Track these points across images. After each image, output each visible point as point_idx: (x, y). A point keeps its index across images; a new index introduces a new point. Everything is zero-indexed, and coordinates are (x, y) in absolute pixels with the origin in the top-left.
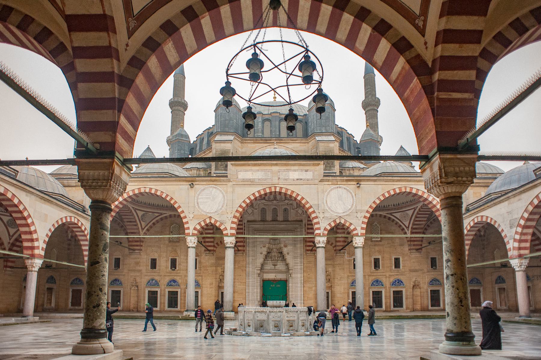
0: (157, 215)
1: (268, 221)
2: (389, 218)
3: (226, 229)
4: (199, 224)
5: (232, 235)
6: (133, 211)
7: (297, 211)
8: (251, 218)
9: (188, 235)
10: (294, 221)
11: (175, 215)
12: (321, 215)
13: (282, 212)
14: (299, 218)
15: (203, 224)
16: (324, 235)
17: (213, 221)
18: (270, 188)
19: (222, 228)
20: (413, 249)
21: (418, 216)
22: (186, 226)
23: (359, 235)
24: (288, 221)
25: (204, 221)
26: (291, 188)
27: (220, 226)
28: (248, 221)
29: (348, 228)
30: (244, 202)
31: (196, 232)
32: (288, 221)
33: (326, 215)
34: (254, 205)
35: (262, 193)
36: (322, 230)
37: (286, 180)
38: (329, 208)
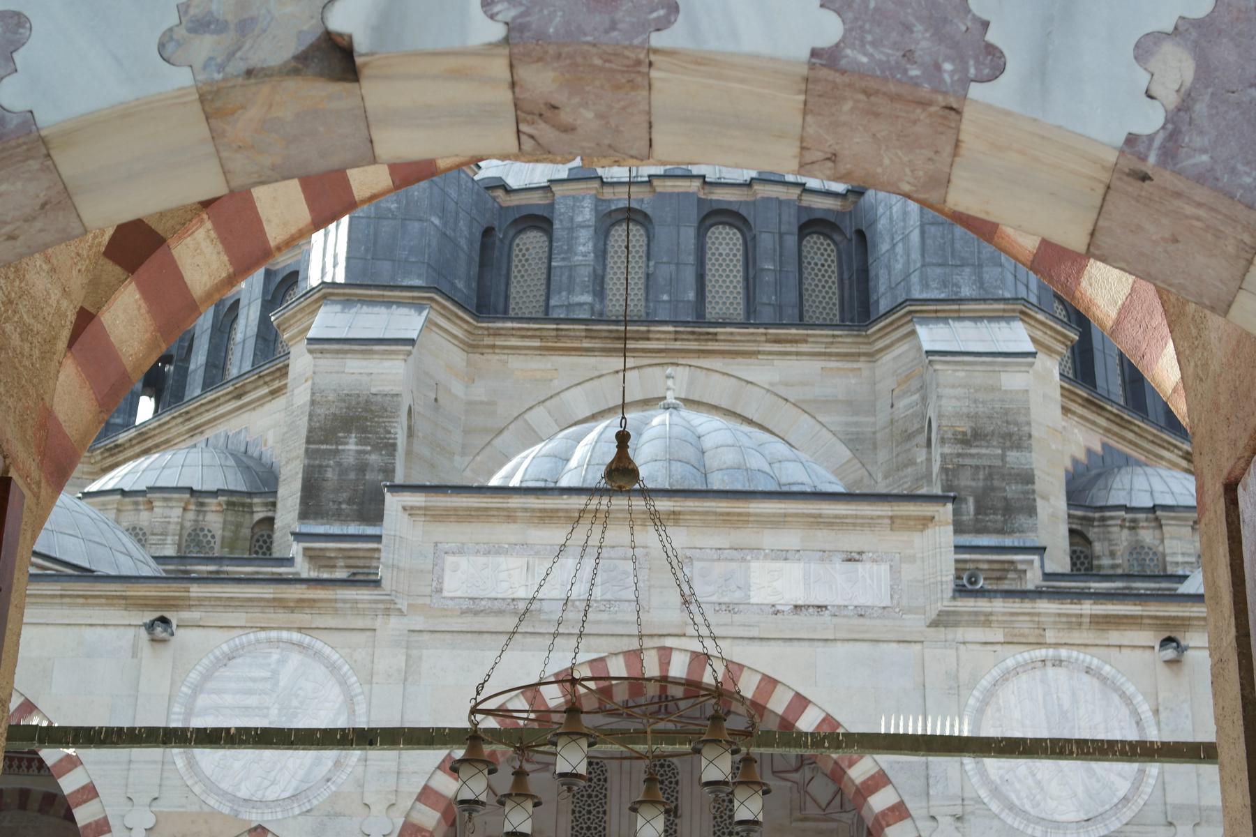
7: (803, 789)
11: (24, 794)
37: (729, 608)
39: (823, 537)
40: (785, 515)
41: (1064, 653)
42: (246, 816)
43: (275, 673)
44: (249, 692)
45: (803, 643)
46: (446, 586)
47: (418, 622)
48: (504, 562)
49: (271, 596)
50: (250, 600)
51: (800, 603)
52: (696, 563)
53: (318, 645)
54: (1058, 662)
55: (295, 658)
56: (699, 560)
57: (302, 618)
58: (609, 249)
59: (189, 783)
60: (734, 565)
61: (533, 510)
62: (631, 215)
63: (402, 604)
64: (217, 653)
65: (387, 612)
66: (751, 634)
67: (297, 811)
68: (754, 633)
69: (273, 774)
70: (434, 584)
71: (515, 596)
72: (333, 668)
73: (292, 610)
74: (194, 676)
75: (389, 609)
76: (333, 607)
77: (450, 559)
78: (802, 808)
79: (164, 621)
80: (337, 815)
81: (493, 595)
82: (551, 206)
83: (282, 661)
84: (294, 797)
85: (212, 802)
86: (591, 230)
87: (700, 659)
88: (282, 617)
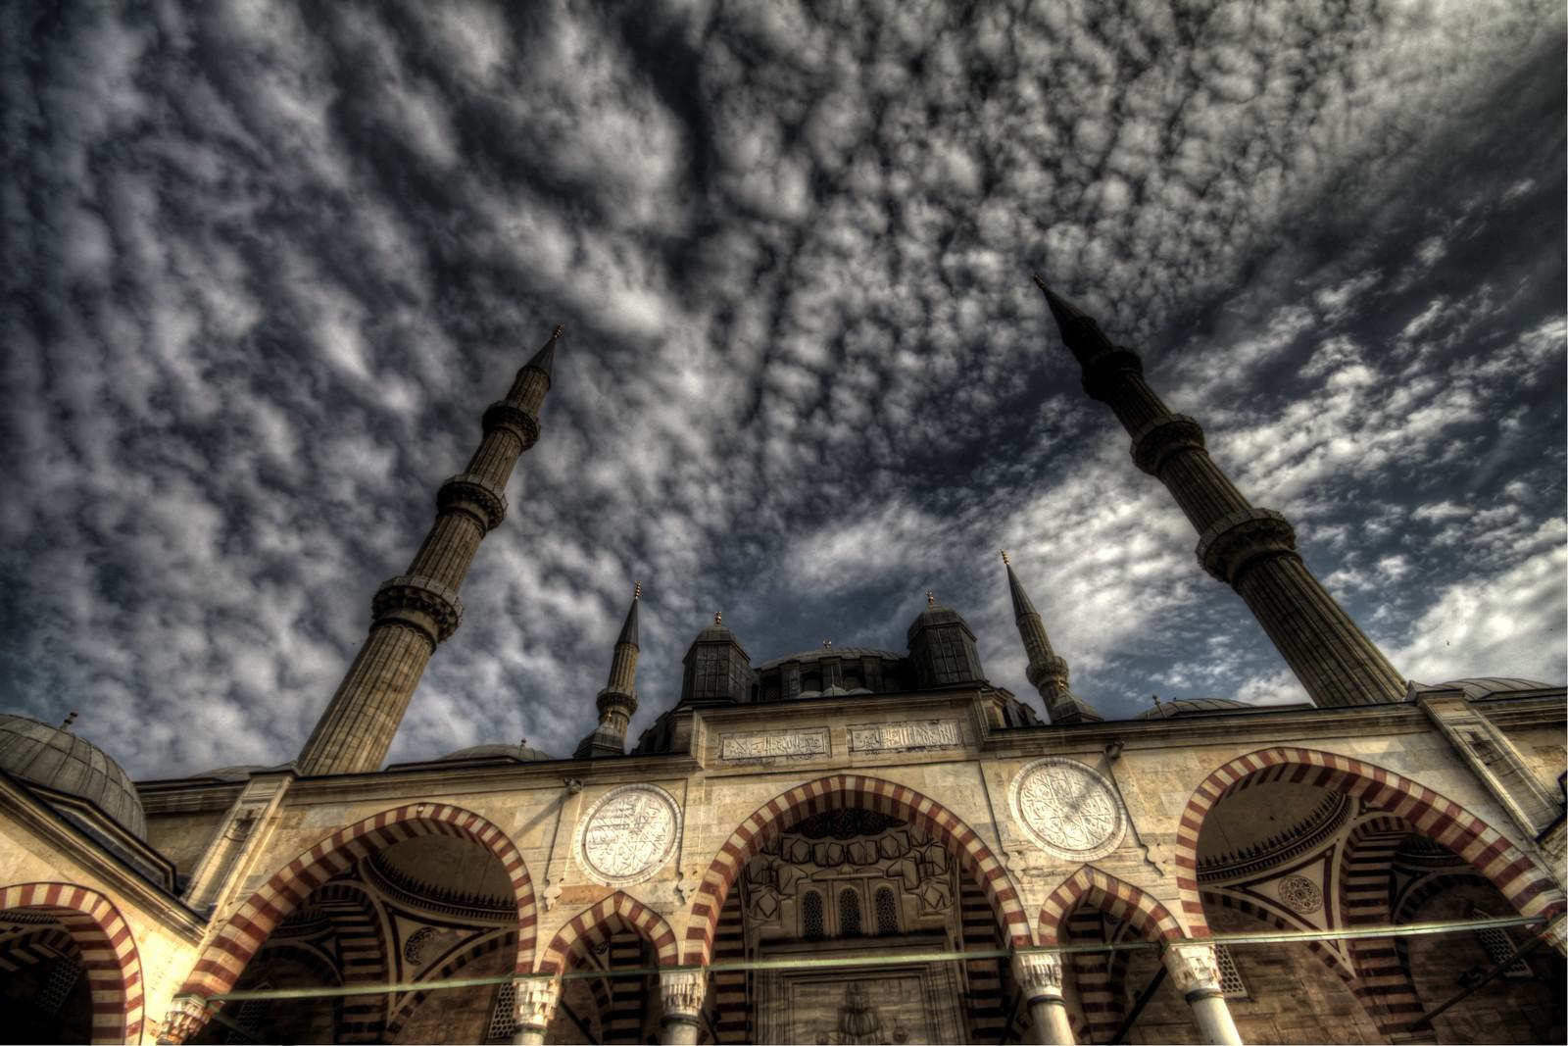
0: (463, 934)
1: (829, 939)
2: (1246, 907)
5: (694, 961)
6: (384, 919)
7: (922, 898)
8: (774, 929)
10: (915, 933)
12: (1016, 864)
13: (874, 905)
14: (930, 920)
15: (588, 921)
16: (1045, 946)
17: (626, 908)
18: (825, 781)
20: (1397, 1028)
21: (1353, 881)
23: (1188, 934)
24: (896, 934)
25: (596, 909)
26: (894, 775)
27: (649, 927)
29: (1132, 907)
32: (896, 934)
33: (1034, 860)
34: (782, 883)
35: (800, 796)
36: (1034, 923)
37: (874, 751)
38: (1038, 835)
41: (1056, 759)
43: (634, 806)
47: (711, 772)
54: (1054, 764)
57: (649, 776)
68: (888, 763)
72: (666, 800)
78: (924, 908)
83: (638, 799)
84: (641, 872)
88: (638, 777)
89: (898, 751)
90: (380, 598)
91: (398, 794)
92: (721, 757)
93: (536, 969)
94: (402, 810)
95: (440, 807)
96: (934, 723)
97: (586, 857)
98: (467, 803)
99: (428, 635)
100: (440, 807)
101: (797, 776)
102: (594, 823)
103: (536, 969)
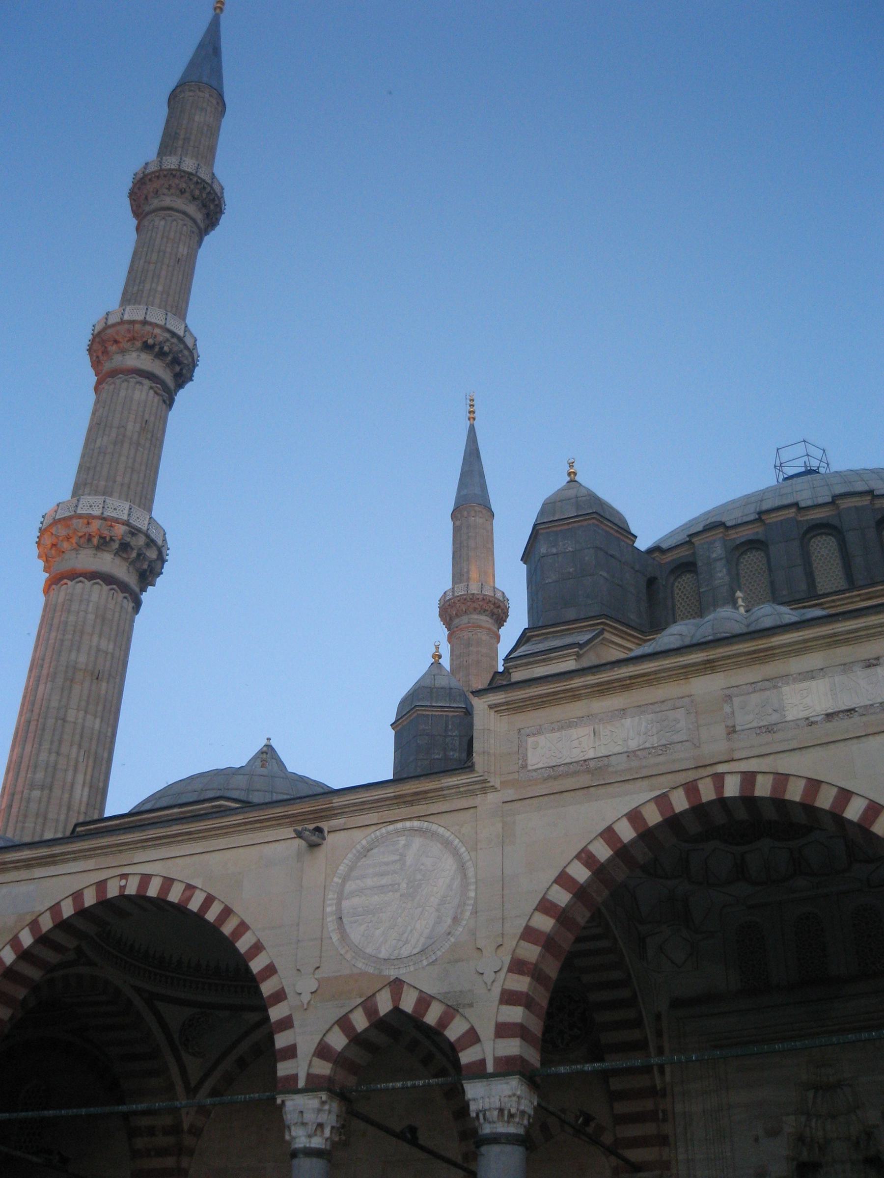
3: (472, 1037)
4: (344, 1023)
5: (508, 1067)
9: (290, 1085)
15: (360, 1022)
17: (408, 1004)
18: (691, 788)
19: (453, 1032)
22: (281, 1041)
26: (801, 766)
28: (677, 1003)
30: (564, 879)
31: (324, 1068)
35: (653, 817)
37: (769, 729)
39: (843, 653)
40: (805, 641)
42: (386, 973)
44: (382, 875)
45: (837, 744)
46: (529, 762)
47: (510, 793)
48: (574, 733)
49: (392, 795)
50: (377, 801)
51: (830, 711)
52: (734, 699)
53: (434, 827)
55: (417, 842)
56: (737, 696)
58: (741, 572)
59: (342, 952)
60: (768, 692)
61: (592, 686)
62: (753, 544)
63: (495, 781)
64: (359, 847)
65: (484, 791)
66: (790, 747)
67: (425, 963)
68: (794, 744)
69: (406, 935)
70: (520, 761)
71: (586, 757)
72: (447, 843)
73: (411, 803)
74: (342, 869)
75: (484, 787)
76: (439, 795)
77: (530, 740)
79: (319, 830)
80: (457, 961)
81: (568, 761)
82: (694, 554)
83: (407, 846)
85: (360, 965)
86: (724, 561)
87: (749, 778)
88: (405, 811)
89: (810, 723)
90: (48, 541)
91: (90, 864)
92: (524, 766)
93: (301, 1084)
94: (101, 886)
95: (146, 879)
96: (871, 664)
97: (344, 936)
98: (172, 870)
99: (124, 587)
100: (146, 879)
101: (646, 783)
102: (350, 886)
103: (301, 1084)
